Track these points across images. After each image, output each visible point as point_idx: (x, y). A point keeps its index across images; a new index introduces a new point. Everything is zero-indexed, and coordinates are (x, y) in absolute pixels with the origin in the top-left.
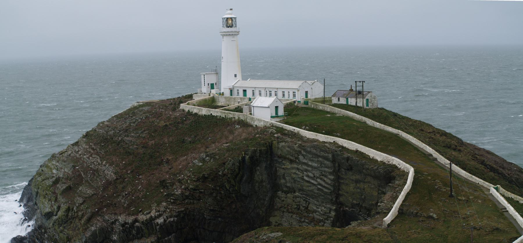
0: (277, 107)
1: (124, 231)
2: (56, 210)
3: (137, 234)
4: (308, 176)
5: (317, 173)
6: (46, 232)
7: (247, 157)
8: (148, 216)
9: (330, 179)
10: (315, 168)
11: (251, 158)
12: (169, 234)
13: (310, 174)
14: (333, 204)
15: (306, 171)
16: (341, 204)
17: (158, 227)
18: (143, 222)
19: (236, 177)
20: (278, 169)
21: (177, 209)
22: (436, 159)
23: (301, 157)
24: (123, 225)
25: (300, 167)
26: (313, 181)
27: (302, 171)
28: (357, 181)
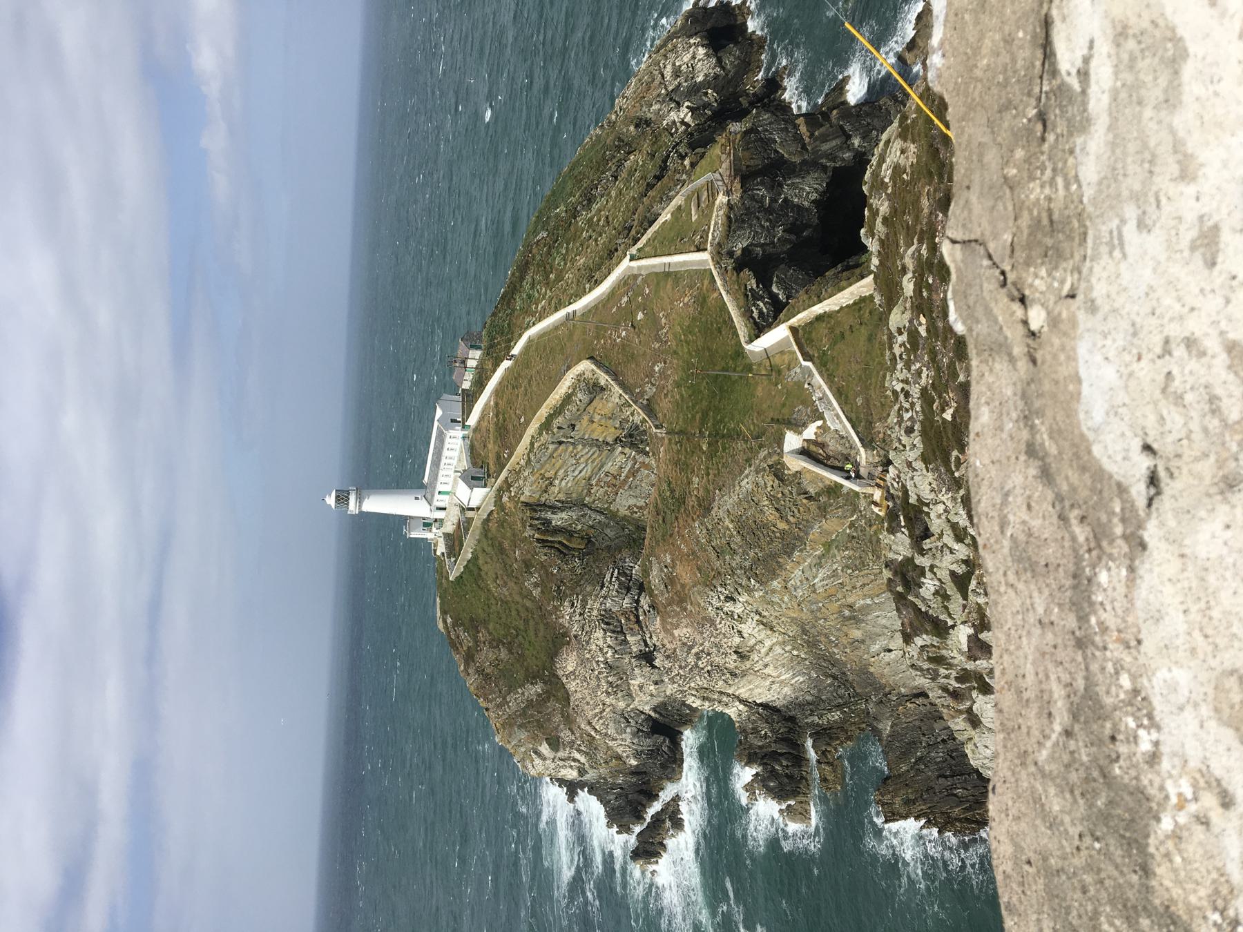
0: (473, 478)
2: (577, 764)
3: (622, 679)
6: (604, 778)
9: (582, 450)
12: (625, 642)
16: (617, 440)
19: (561, 552)
22: (575, 312)
23: (547, 475)
24: (608, 694)
26: (580, 468)
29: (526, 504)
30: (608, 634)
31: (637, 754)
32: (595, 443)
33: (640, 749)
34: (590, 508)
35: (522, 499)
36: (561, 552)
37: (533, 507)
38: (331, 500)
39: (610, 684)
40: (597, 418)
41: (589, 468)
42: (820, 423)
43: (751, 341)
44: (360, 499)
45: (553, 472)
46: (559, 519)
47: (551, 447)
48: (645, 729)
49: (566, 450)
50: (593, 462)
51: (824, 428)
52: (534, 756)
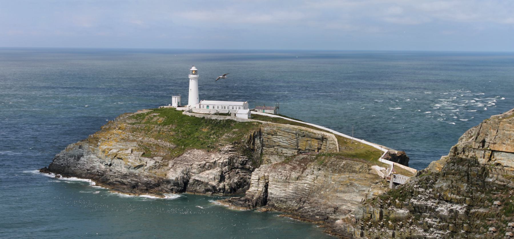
1: (201, 167)
4: (283, 140)
5: (287, 139)
7: (252, 134)
8: (214, 160)
10: (287, 137)
11: (254, 134)
12: (225, 166)
13: (284, 139)
14: (296, 149)
15: (282, 138)
16: (300, 150)
17: (220, 164)
18: (212, 163)
20: (264, 138)
21: (227, 156)
23: (278, 134)
25: (278, 137)
27: (279, 138)
28: (307, 141)
29: (260, 129)
30: (228, 160)
31: (177, 179)
32: (298, 143)
33: (179, 179)
34: (262, 149)
35: (262, 128)
36: (249, 142)
37: (260, 133)
38: (194, 69)
39: (205, 165)
40: (310, 142)
41: (285, 144)
42: (385, 169)
43: (382, 158)
44: (194, 79)
45: (280, 134)
46: (257, 141)
47: (294, 132)
48: (185, 180)
49: (293, 136)
50: (290, 145)
51: (386, 170)
52: (130, 150)
